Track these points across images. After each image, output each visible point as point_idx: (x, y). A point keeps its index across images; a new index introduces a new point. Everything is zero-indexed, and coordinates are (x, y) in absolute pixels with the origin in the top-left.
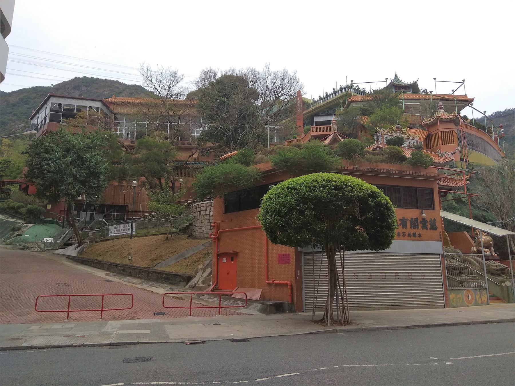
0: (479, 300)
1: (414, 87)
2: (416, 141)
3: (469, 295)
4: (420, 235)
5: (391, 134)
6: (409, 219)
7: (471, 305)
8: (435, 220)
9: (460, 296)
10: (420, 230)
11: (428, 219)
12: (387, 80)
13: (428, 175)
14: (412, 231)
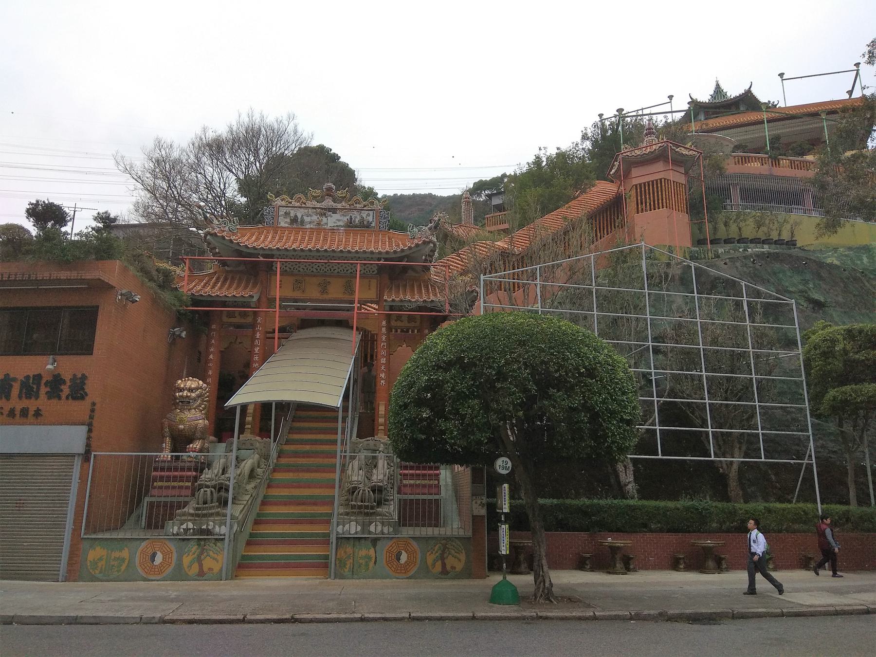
0: (190, 566)
1: (748, 101)
2: (371, 213)
3: (159, 553)
4: (38, 413)
5: (305, 204)
6: (21, 377)
7: (158, 578)
8: (84, 377)
9: (125, 554)
10: (42, 401)
11: (67, 377)
12: (671, 99)
13: (55, 278)
14: (19, 406)
